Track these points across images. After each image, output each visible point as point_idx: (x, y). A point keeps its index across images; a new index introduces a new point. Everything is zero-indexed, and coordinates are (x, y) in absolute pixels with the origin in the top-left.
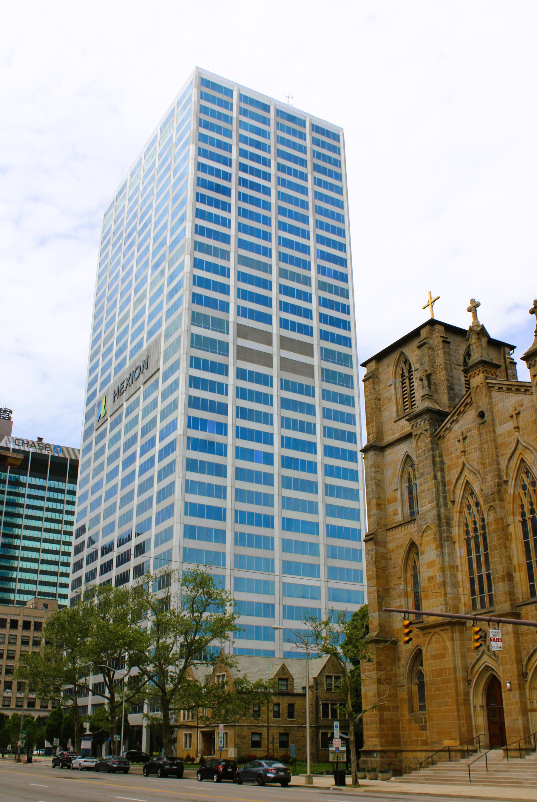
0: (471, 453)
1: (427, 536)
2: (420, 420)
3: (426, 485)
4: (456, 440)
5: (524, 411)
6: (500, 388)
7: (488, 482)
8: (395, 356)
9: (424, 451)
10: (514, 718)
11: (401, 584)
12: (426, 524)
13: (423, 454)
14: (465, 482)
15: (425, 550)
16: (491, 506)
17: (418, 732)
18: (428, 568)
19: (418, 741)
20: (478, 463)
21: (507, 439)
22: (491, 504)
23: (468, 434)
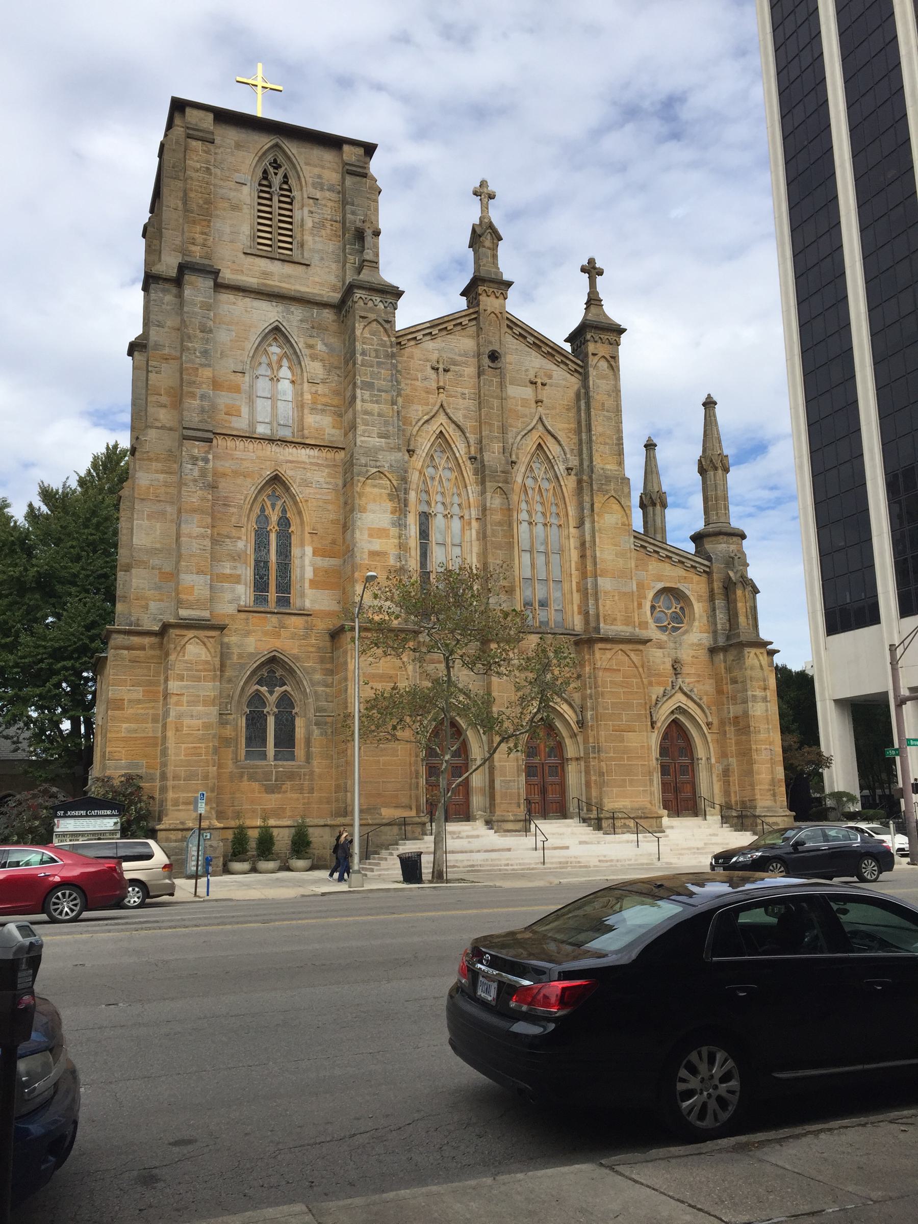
0: (455, 397)
1: (375, 486)
2: (379, 299)
3: (376, 406)
4: (429, 364)
5: (551, 386)
6: (521, 335)
7: (494, 453)
8: (265, 141)
9: (376, 350)
10: (508, 779)
11: (239, 538)
12: (378, 467)
13: (373, 354)
14: (437, 432)
15: (369, 507)
16: (499, 487)
17: (257, 795)
18: (371, 536)
19: (254, 811)
20: (465, 417)
21: (519, 408)
22: (500, 485)
23: (452, 368)
